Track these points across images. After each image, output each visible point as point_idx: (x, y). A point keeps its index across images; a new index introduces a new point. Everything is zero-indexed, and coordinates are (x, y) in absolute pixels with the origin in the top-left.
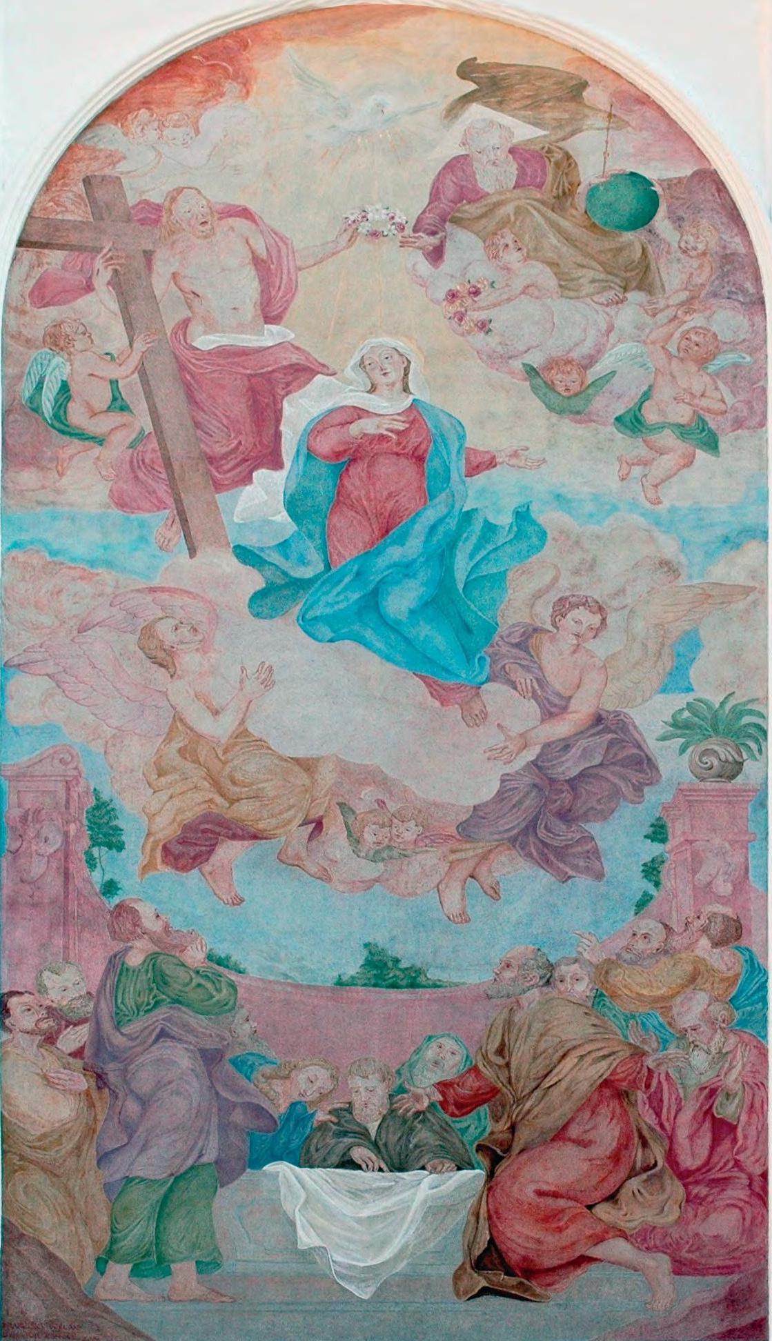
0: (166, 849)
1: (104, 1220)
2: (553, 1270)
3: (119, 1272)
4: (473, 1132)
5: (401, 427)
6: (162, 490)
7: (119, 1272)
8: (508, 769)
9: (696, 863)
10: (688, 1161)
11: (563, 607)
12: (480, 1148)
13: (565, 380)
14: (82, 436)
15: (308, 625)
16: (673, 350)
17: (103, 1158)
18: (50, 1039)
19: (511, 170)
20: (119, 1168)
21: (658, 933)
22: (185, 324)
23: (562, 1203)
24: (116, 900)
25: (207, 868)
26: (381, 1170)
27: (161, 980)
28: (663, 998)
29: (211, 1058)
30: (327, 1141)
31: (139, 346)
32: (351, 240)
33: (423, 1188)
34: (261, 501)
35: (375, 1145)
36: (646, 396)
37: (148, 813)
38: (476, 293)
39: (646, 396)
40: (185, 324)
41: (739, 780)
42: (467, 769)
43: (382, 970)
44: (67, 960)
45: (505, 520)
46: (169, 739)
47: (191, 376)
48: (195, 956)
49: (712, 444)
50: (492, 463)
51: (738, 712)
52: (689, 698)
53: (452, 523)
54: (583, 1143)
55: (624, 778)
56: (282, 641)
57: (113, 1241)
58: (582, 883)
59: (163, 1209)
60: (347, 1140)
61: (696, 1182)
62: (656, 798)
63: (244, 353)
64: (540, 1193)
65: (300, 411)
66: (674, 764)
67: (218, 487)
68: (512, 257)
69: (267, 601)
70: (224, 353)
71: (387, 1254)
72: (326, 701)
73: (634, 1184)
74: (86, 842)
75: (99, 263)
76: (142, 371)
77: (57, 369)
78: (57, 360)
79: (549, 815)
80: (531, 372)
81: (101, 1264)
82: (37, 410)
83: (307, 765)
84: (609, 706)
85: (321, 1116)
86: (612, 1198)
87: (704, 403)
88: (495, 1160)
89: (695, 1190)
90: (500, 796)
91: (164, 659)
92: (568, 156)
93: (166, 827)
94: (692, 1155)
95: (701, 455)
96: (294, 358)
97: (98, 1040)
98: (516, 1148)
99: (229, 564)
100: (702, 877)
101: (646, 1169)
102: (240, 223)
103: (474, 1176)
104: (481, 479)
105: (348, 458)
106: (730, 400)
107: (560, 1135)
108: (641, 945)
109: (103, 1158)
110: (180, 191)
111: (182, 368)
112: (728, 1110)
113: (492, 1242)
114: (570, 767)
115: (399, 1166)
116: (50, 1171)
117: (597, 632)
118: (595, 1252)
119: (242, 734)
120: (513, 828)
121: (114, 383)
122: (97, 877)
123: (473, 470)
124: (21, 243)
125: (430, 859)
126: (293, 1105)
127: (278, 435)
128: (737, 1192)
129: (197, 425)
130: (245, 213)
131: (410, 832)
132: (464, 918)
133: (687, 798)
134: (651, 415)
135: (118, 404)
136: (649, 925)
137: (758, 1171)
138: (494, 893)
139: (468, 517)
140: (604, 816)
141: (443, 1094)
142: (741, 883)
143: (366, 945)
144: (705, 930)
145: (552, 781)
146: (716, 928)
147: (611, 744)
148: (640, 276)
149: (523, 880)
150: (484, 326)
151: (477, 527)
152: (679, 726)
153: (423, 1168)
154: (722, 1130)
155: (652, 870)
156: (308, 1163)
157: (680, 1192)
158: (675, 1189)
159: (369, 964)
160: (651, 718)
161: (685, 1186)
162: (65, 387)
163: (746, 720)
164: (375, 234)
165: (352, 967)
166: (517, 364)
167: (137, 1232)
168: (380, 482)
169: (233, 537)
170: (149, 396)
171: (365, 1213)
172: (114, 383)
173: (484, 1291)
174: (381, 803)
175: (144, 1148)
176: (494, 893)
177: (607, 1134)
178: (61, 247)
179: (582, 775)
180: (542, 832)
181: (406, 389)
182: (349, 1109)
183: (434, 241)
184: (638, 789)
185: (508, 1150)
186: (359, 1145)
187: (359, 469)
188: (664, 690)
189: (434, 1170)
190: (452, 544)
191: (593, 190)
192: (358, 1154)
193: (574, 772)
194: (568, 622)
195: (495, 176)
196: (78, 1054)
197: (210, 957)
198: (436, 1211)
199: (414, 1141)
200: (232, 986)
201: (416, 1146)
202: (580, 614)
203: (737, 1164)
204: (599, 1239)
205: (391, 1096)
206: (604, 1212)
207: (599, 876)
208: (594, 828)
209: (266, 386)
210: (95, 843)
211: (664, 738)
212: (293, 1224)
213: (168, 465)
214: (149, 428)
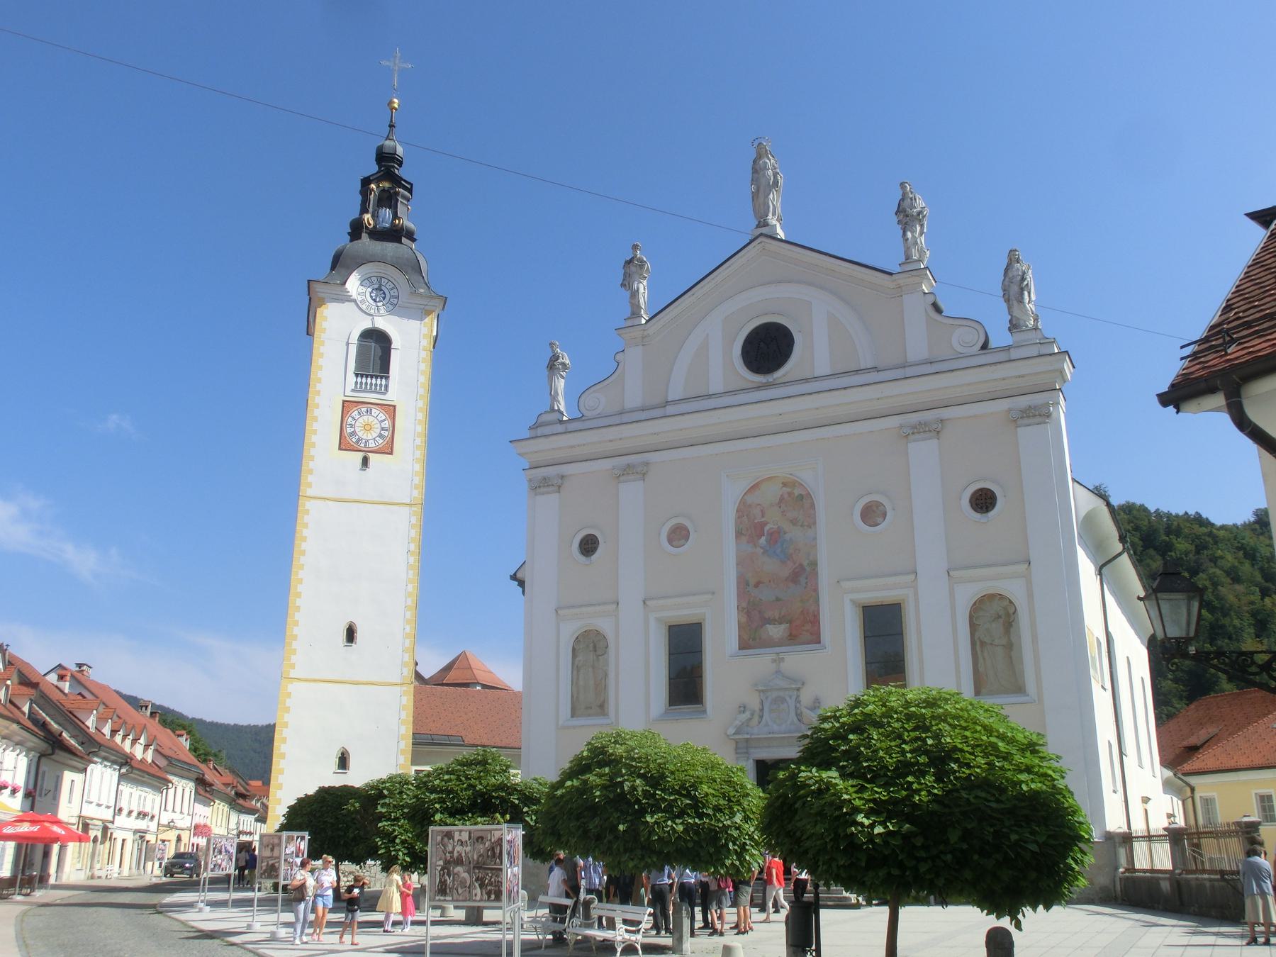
30: (772, 621)
33: (783, 626)
34: (763, 540)
37: (752, 582)
43: (778, 599)
65: (767, 528)
66: (808, 569)
79: (795, 577)
105: (771, 534)
160: (805, 564)
168: (776, 537)
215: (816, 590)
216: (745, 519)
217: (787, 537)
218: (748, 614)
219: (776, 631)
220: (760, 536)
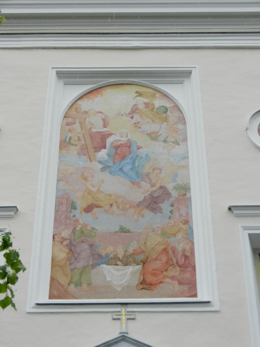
0: (84, 210)
1: (70, 276)
2: (156, 284)
3: (72, 286)
4: (140, 259)
5: (126, 142)
6: (86, 152)
8: (145, 195)
9: (179, 210)
10: (180, 263)
11: (154, 170)
12: (141, 261)
13: (153, 135)
14: (73, 145)
15: (110, 173)
16: (171, 130)
17: (71, 264)
18: (62, 242)
19: (144, 106)
20: (73, 267)
21: (173, 223)
22: (91, 128)
23: (157, 272)
24: (75, 218)
25: (92, 212)
26: (122, 266)
27: (82, 232)
28: (174, 234)
29: (91, 246)
30: (113, 261)
31: (83, 131)
32: (118, 116)
33: (130, 269)
34: (103, 154)
35: (121, 261)
36: (167, 137)
37: (81, 204)
38: (139, 123)
39: (167, 137)
40: (91, 128)
41: (186, 197)
42: (138, 195)
43: (123, 230)
44: (65, 228)
45: (144, 156)
46: (85, 191)
47: (92, 136)
48: (89, 228)
49: (178, 144)
50: (142, 148)
51: (185, 185)
52: (176, 183)
53: (135, 157)
55: (166, 196)
56: (106, 176)
57: (72, 280)
58: (159, 214)
59: (81, 274)
60: (116, 260)
61: (182, 267)
62: (171, 200)
63: (100, 132)
64: (153, 270)
65: (109, 141)
66: (174, 194)
67: (96, 152)
68: (144, 118)
69: (103, 170)
70: (97, 132)
71: (123, 282)
72: (113, 185)
73: (170, 268)
74: (70, 209)
75: (77, 120)
76: (83, 135)
77: (70, 135)
78: (70, 134)
79: (153, 203)
80: (148, 134)
81: (69, 284)
82: (66, 141)
83: (110, 195)
84: (163, 185)
85: (112, 256)
86: (166, 270)
87: (177, 138)
88: (144, 263)
89: (182, 269)
90: (144, 200)
91: (86, 179)
92: (153, 104)
93: (85, 206)
95: (177, 146)
96: (109, 133)
97: (71, 242)
98: (148, 261)
99: (96, 163)
100: (180, 213)
101: (173, 265)
102: (100, 114)
103: (140, 267)
104: (140, 150)
105: (117, 147)
106: (181, 138)
107: (156, 259)
108: (170, 225)
109: (71, 264)
110: (91, 109)
111: (90, 135)
112: (188, 254)
113: (144, 279)
114: (156, 195)
115: (126, 265)
116: (60, 266)
117: (160, 173)
118: (163, 281)
119: (98, 190)
120: (146, 205)
121: (79, 137)
122: (72, 215)
123: (138, 149)
124: (65, 117)
125: (132, 210)
126: (106, 254)
127: (106, 144)
128: (190, 269)
129: (92, 143)
130: (101, 112)
131: (128, 206)
132: (138, 220)
133: (177, 200)
134: (168, 140)
135: (79, 140)
136: (171, 221)
137: (193, 265)
138: (143, 216)
139: (138, 156)
140: (162, 203)
141: (134, 251)
142: (187, 214)
143: (121, 226)
144: (181, 222)
145: (153, 197)
146: (183, 221)
147: (164, 191)
148: (166, 120)
149: (148, 214)
150: (140, 128)
151: (139, 157)
152: (175, 188)
153: (130, 265)
154: (186, 257)
155: (171, 212)
156: (108, 264)
158: (178, 269)
159: (120, 229)
160: (170, 187)
161: (180, 268)
162: (70, 138)
163: (187, 187)
164: (122, 115)
165: (117, 229)
166: (145, 133)
167: (76, 278)
168: (122, 151)
169: (98, 160)
170: (84, 139)
171: (120, 274)
172: (79, 137)
173: (142, 288)
174: (123, 201)
175: (78, 262)
176: (143, 216)
177: (164, 258)
178: (71, 118)
179: (158, 196)
180: (151, 205)
181: (127, 137)
182: (117, 254)
183: (132, 116)
184: (168, 198)
185: (146, 261)
186: (118, 261)
187: (119, 149)
188: (172, 182)
189: (132, 266)
190: (135, 159)
191: (157, 109)
192: (119, 263)
193: (157, 196)
194: (155, 172)
195: (141, 106)
196: (67, 245)
197: (92, 228)
198: (133, 274)
199: (129, 260)
200: (95, 233)
201: (129, 261)
202: (157, 170)
203: (190, 264)
205: (125, 252)
206: (165, 273)
207: (162, 213)
208: (161, 205)
209: (104, 137)
210: (72, 209)
211: (172, 190)
212: (106, 276)
213: (87, 148)
214: (84, 143)
215: (187, 222)
216: (77, 126)
217: (143, 152)
218: (71, 247)
220: (98, 149)
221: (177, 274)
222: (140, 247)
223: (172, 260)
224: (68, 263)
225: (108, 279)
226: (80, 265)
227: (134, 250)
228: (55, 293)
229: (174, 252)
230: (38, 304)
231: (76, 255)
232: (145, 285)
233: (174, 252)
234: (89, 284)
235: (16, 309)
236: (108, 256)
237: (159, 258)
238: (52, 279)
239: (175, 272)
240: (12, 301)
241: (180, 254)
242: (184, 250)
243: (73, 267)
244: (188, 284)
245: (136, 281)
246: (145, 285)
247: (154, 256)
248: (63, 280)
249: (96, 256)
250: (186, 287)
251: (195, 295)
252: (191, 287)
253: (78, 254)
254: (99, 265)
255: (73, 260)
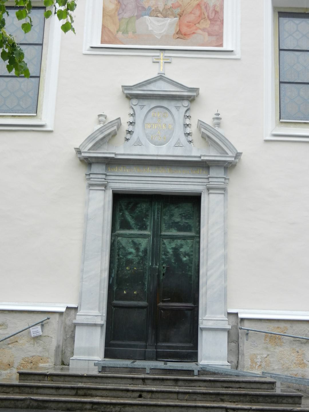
2: (189, 34)
3: (120, 33)
4: (177, 12)
7: (120, 33)
10: (211, 17)
12: (178, 14)
17: (119, 14)
20: (121, 16)
23: (191, 24)
26: (162, 17)
30: (155, 13)
33: (169, 21)
35: (161, 14)
54: (194, 14)
57: (120, 28)
59: (127, 24)
60: (157, 13)
61: (212, 21)
64: (188, 22)
71: (162, 32)
73: (202, 21)
81: (117, 31)
85: (153, 8)
86: (199, 23)
88: (180, 16)
89: (212, 22)
94: (212, 16)
98: (184, 14)
101: (204, 18)
103: (177, 19)
107: (191, 13)
109: (119, 14)
112: (218, 9)
113: (179, 30)
115: (165, 17)
116: (110, 16)
126: (149, 7)
128: (219, 23)
137: (222, 19)
141: (173, 5)
153: (169, 17)
154: (216, 12)
156: (151, 16)
157: (209, 22)
158: (209, 22)
161: (210, 21)
171: (159, 24)
173: (178, 38)
175: (125, 13)
177: (198, 13)
182: (158, 8)
186: (158, 13)
189: (171, 18)
192: (159, 15)
199: (168, 13)
201: (168, 14)
203: (219, 18)
204: (196, 29)
205: (164, 6)
206: (197, 25)
212: (148, 26)
219: (160, 26)
221: (208, 26)
222: (178, 2)
223: (204, 15)
224: (117, 13)
225: (150, 28)
226: (126, 15)
227: (173, 4)
228: (106, 39)
229: (206, 7)
230: (92, 47)
231: (123, 6)
232: (181, 35)
233: (206, 7)
234: (134, 32)
235: (75, 33)
236: (150, 9)
237: (193, 12)
238: (104, 27)
239: (206, 24)
240: (72, 26)
241: (211, 9)
242: (215, 6)
243: (121, 16)
244: (216, 35)
245: (173, 31)
246: (181, 35)
247: (189, 10)
248: (112, 28)
249: (140, 8)
250: (214, 38)
251: (221, 45)
252: (218, 37)
253: (125, 6)
254: (142, 16)
255: (121, 12)
